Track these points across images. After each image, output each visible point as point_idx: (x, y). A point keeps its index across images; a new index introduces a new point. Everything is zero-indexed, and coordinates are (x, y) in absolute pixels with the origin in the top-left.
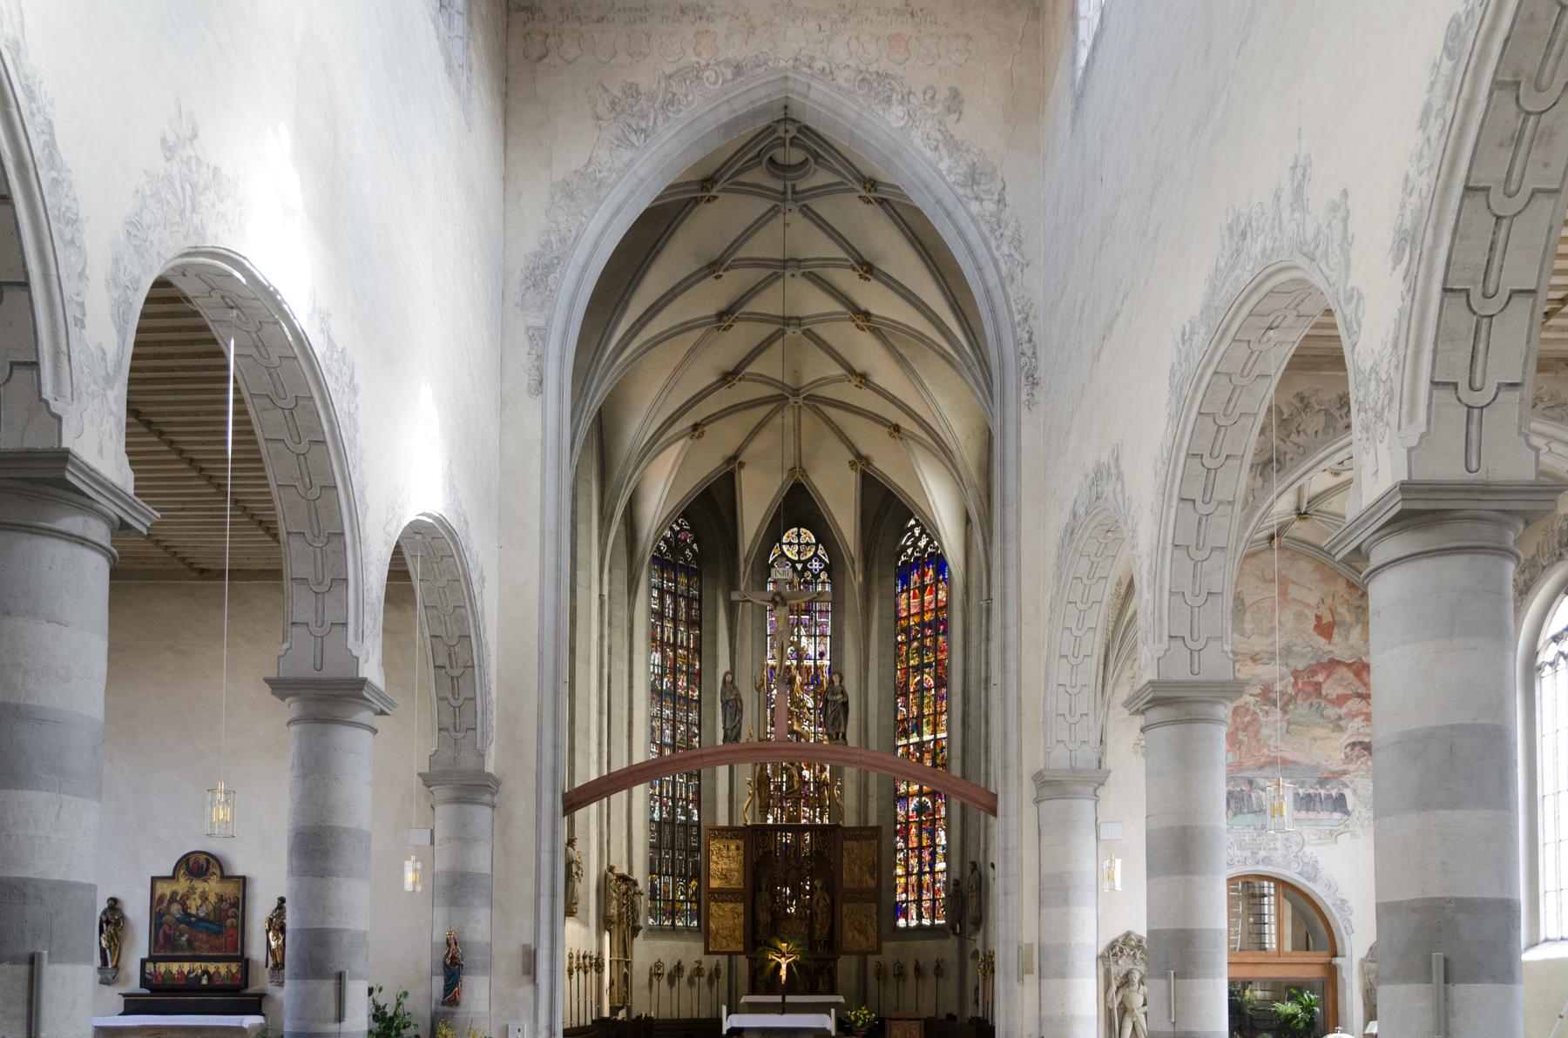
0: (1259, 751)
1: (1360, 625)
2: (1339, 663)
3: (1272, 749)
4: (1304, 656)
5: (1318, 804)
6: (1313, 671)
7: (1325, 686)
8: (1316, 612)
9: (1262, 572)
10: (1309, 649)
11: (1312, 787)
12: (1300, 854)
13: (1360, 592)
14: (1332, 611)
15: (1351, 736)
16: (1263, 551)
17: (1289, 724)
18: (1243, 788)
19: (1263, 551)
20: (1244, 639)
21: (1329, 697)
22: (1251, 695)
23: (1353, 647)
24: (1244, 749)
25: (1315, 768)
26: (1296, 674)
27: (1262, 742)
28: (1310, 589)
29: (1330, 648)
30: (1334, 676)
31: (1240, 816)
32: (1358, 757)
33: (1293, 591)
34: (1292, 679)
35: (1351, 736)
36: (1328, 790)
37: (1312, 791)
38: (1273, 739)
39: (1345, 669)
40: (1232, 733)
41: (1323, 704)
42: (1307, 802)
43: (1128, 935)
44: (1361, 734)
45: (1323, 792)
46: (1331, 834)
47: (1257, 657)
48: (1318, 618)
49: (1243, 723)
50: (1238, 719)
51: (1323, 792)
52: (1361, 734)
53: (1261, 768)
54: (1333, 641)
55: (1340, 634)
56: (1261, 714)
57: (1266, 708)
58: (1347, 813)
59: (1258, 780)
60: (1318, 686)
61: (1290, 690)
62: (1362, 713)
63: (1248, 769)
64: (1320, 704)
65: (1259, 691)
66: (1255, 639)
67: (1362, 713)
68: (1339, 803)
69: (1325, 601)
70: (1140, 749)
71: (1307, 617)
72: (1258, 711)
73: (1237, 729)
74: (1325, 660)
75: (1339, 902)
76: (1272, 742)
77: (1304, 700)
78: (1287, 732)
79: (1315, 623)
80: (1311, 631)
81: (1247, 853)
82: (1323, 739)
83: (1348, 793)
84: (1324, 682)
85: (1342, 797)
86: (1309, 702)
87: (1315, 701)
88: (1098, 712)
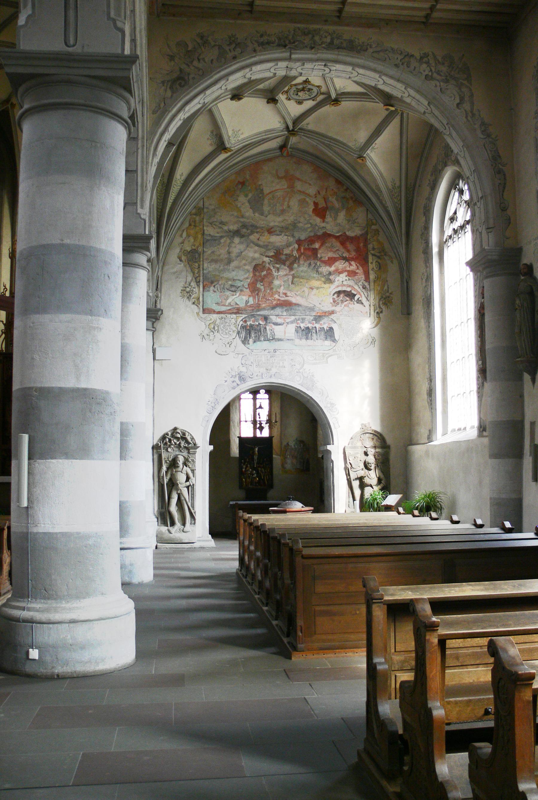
0: (272, 296)
1: (345, 210)
2: (330, 235)
3: (281, 295)
4: (305, 230)
5: (314, 335)
6: (311, 240)
7: (320, 251)
8: (314, 199)
9: (277, 171)
10: (309, 225)
11: (310, 323)
12: (301, 371)
13: (345, 187)
14: (326, 200)
15: (338, 286)
16: (277, 157)
17: (294, 277)
18: (261, 322)
19: (277, 157)
20: (263, 217)
21: (323, 259)
22: (266, 256)
23: (339, 225)
24: (261, 295)
25: (312, 309)
26: (299, 242)
27: (274, 290)
28: (310, 184)
29: (323, 225)
30: (327, 244)
31: (258, 343)
32: (342, 301)
33: (298, 186)
34: (296, 246)
35: (338, 286)
36: (321, 324)
37: (310, 326)
38: (282, 288)
39: (334, 240)
40: (253, 283)
41: (318, 264)
42: (307, 332)
43: (175, 429)
44: (345, 285)
45: (318, 326)
46: (323, 356)
47: (272, 230)
48: (316, 204)
49: (260, 276)
50: (257, 274)
51: (318, 326)
52: (345, 285)
53: (273, 308)
54: (326, 220)
55: (331, 216)
56: (273, 270)
57: (278, 266)
58: (334, 341)
59: (271, 317)
60: (315, 252)
61: (295, 253)
62: (346, 271)
63: (264, 309)
64: (316, 264)
65: (272, 254)
66: (270, 218)
67: (346, 271)
68: (329, 333)
69: (321, 193)
70: (186, 294)
71: (307, 202)
72: (272, 268)
73: (257, 280)
74: (320, 233)
75: (329, 405)
76: (282, 290)
77: (305, 261)
78: (292, 283)
79: (313, 207)
80: (311, 213)
81: (263, 370)
82: (318, 288)
83: (335, 327)
84: (320, 247)
85: (331, 329)
86: (308, 262)
87: (312, 262)
88: (154, 267)
